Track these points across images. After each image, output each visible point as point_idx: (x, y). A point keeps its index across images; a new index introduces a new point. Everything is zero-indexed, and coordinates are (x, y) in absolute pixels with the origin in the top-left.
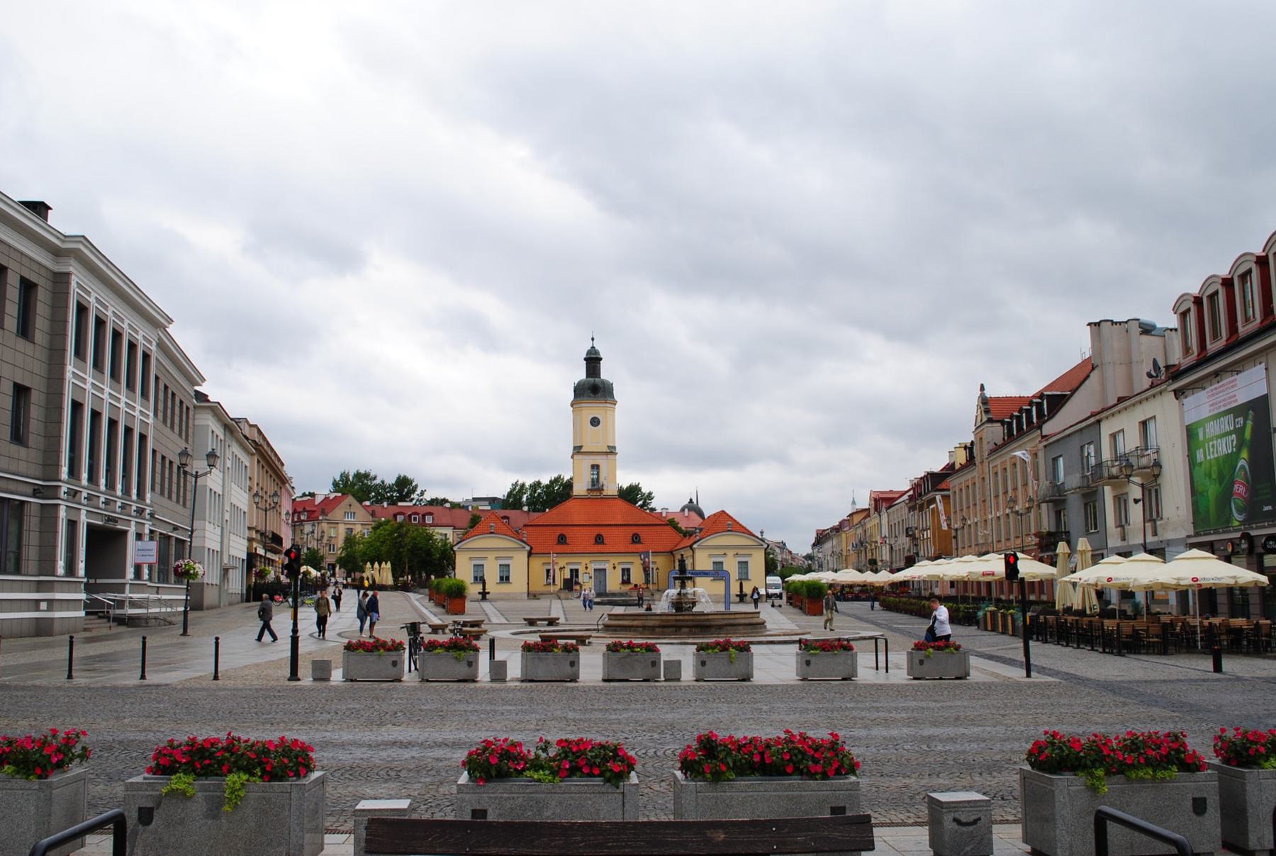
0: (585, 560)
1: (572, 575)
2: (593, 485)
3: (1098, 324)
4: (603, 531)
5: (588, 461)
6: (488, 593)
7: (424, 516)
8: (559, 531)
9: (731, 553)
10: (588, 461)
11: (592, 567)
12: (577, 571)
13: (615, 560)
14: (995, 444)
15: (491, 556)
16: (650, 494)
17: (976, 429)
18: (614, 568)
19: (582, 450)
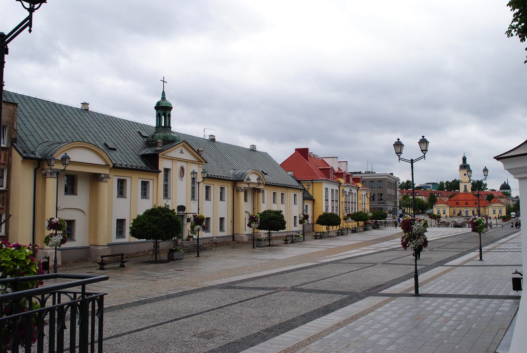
0: (463, 208)
1: (460, 212)
2: (465, 190)
4: (468, 202)
7: (416, 193)
9: (497, 208)
11: (465, 210)
12: (461, 211)
13: (471, 208)
15: (441, 208)
16: (486, 184)
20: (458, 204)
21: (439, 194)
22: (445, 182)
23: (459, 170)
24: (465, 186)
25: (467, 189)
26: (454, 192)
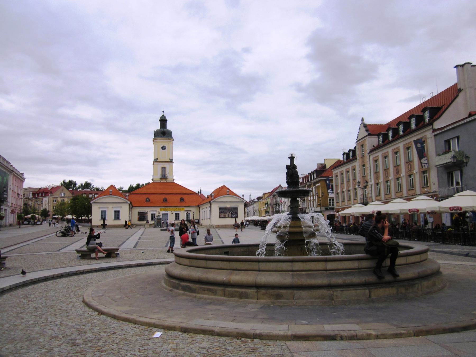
0: (158, 209)
2: (162, 176)
4: (167, 197)
5: (160, 166)
6: (107, 225)
8: (146, 196)
10: (160, 166)
11: (162, 213)
12: (155, 214)
14: (373, 146)
15: (110, 206)
17: (357, 142)
19: (157, 161)
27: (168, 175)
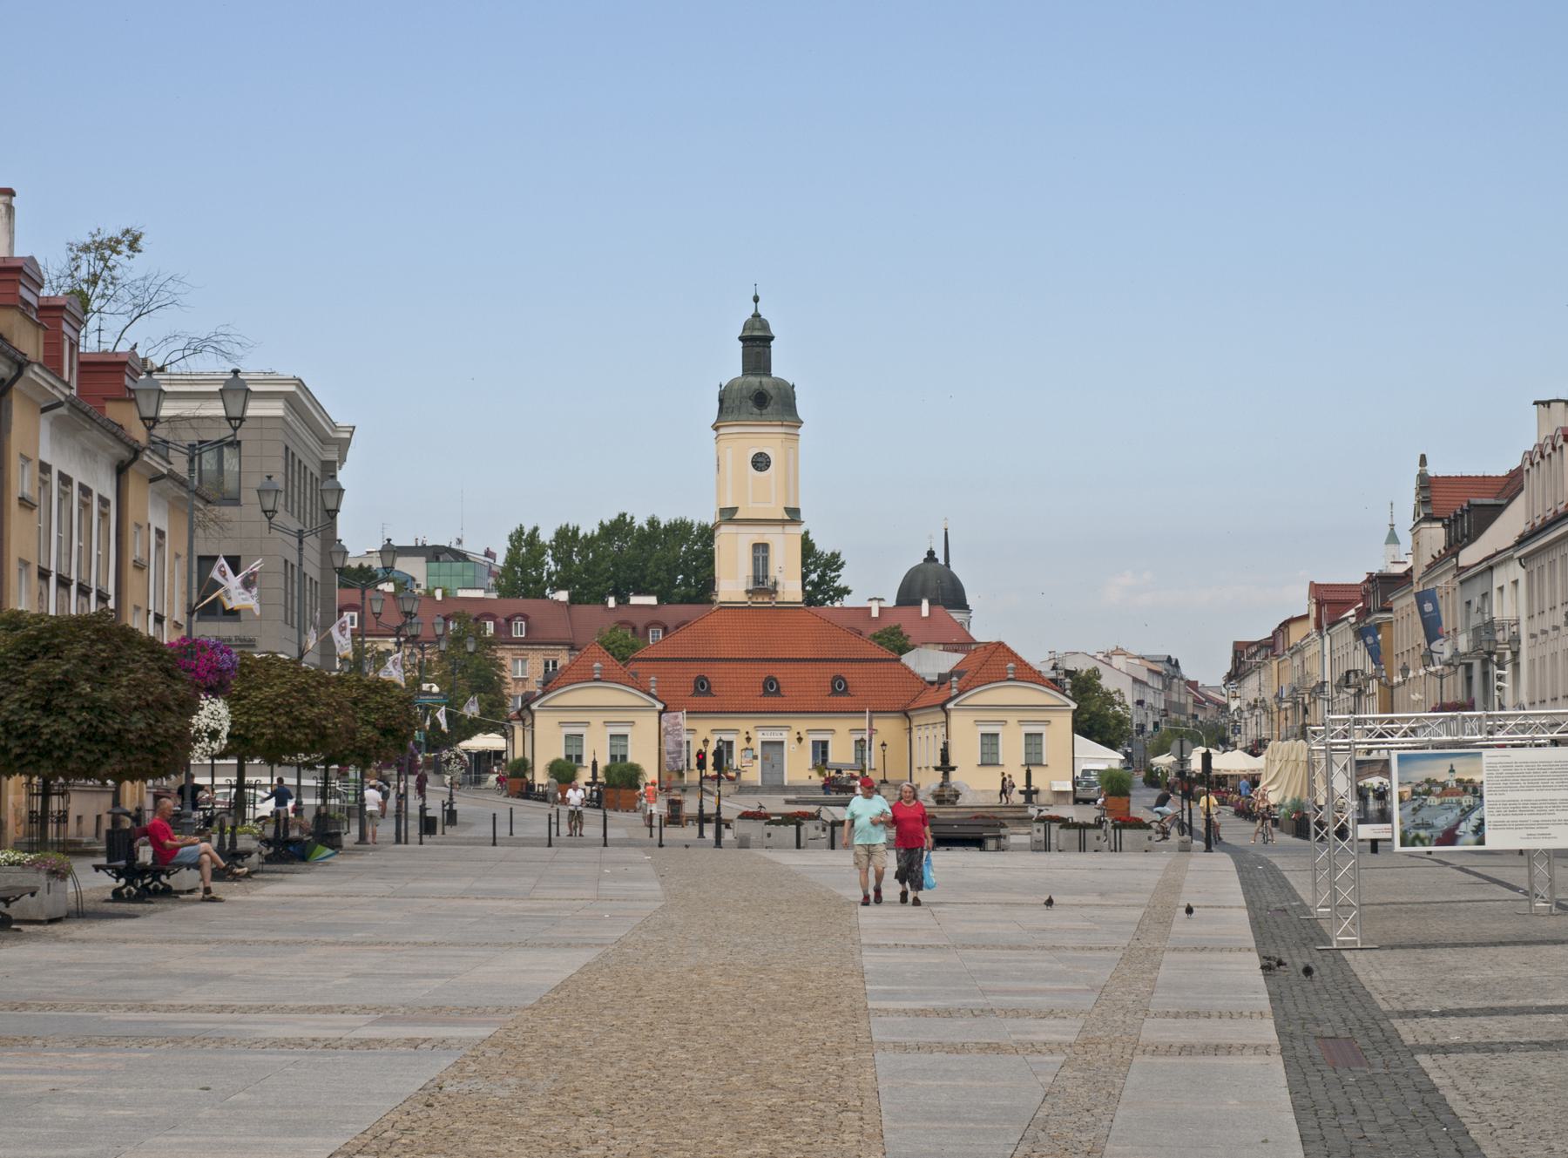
0: (745, 725)
2: (756, 580)
3: (1547, 403)
4: (779, 672)
8: (695, 670)
9: (1012, 718)
11: (759, 737)
12: (730, 744)
13: (801, 725)
15: (596, 719)
16: (835, 556)
18: (800, 740)
20: (709, 692)
21: (509, 620)
22: (546, 536)
23: (716, 428)
24: (756, 546)
25: (774, 572)
26: (624, 615)
27: (780, 579)
